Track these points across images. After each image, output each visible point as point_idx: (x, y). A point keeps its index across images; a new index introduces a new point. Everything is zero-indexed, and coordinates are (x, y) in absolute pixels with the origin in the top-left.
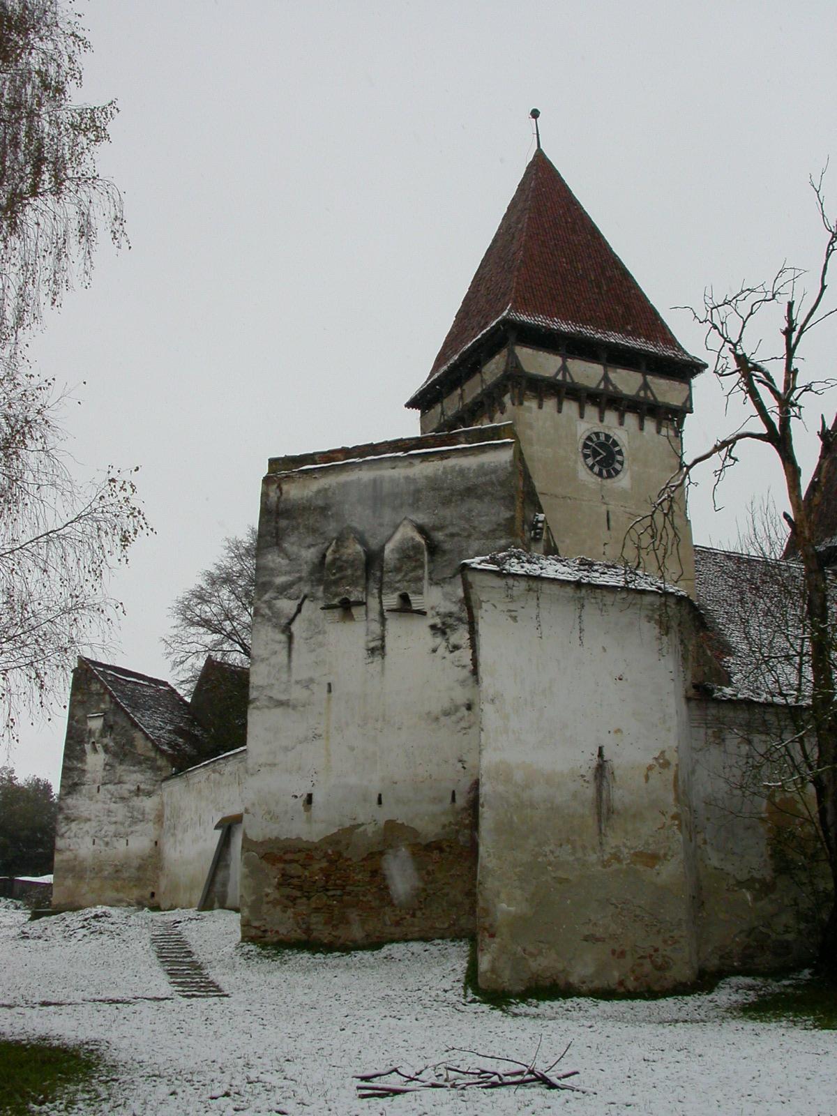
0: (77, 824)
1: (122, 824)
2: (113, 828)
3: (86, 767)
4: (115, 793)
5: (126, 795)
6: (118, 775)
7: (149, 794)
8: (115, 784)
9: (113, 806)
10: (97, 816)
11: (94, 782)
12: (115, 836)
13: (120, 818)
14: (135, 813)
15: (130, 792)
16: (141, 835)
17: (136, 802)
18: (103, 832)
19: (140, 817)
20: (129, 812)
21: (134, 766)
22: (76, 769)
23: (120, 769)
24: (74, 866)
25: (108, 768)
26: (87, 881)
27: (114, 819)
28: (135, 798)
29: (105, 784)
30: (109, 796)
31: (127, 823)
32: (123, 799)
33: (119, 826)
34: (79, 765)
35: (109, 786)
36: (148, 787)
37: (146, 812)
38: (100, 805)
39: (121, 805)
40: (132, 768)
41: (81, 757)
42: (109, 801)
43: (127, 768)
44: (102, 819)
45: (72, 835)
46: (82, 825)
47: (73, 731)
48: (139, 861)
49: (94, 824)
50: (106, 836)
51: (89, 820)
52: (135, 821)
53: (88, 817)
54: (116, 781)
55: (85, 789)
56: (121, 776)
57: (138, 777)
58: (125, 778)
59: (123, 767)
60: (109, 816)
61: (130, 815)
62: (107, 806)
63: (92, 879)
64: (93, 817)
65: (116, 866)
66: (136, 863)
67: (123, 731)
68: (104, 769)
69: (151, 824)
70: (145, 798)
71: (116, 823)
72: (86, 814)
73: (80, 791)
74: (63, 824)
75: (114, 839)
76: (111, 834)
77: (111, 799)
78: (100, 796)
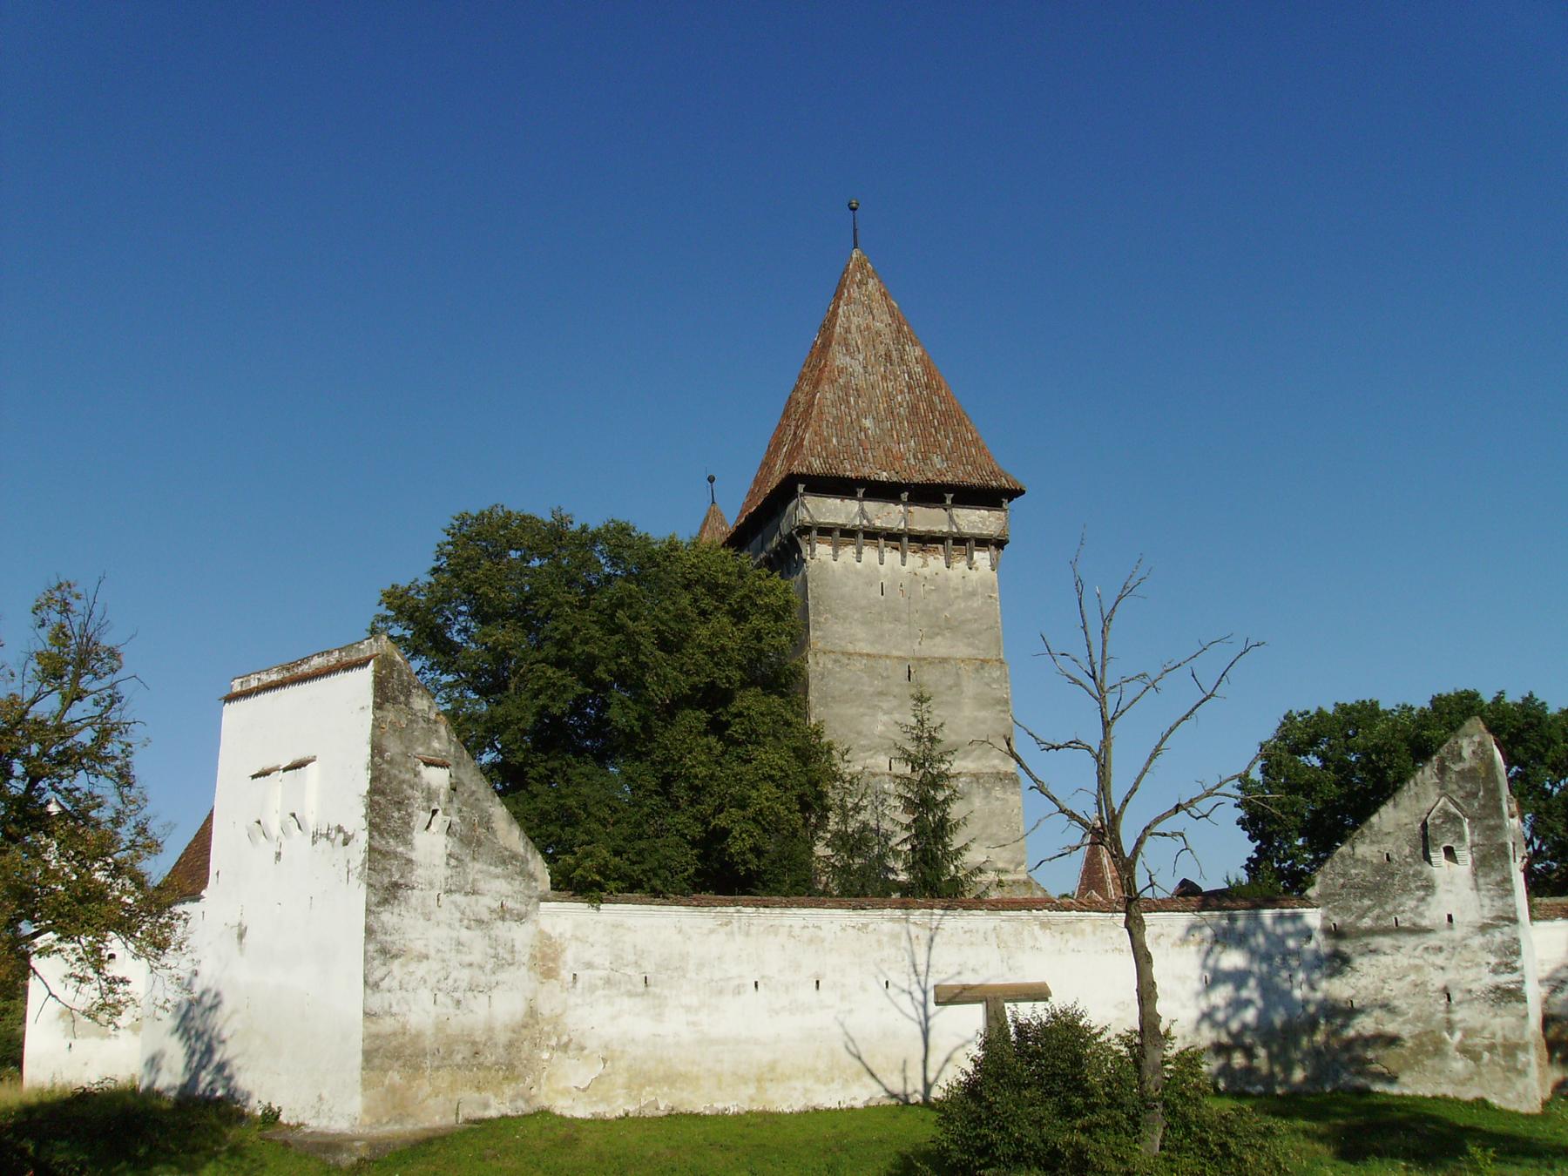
0: (402, 965)
1: (481, 968)
2: (465, 975)
3: (413, 855)
4: (467, 910)
5: (485, 916)
6: (470, 879)
7: (521, 918)
8: (467, 894)
9: (465, 934)
10: (439, 951)
11: (431, 885)
12: (471, 990)
13: (476, 957)
14: (501, 950)
15: (492, 911)
16: (511, 989)
17: (502, 929)
18: (450, 981)
19: (508, 957)
20: (491, 947)
21: (496, 867)
22: (396, 855)
23: (475, 868)
24: (402, 1045)
25: (453, 862)
26: (427, 1073)
27: (467, 959)
28: (499, 923)
29: (449, 891)
30: (458, 915)
31: (488, 967)
32: (480, 922)
33: (477, 972)
34: (400, 849)
35: (457, 897)
36: (518, 906)
37: (516, 948)
38: (443, 932)
39: (479, 933)
40: (492, 868)
41: (403, 833)
42: (457, 925)
43: (485, 867)
44: (447, 956)
45: (395, 984)
46: (413, 967)
47: (385, 779)
48: (510, 1035)
49: (434, 964)
50: (455, 990)
51: (427, 957)
52: (501, 964)
53: (424, 951)
54: (468, 888)
55: (415, 896)
56: (474, 880)
57: (502, 886)
58: (481, 885)
59: (478, 866)
60: (458, 951)
61: (492, 952)
62: (454, 934)
63: (438, 1068)
64: (432, 953)
65: (474, 1043)
66: (502, 1038)
67: (472, 800)
68: (448, 864)
69: (524, 970)
70: (514, 924)
71: (471, 965)
72: (419, 946)
73: (406, 900)
74: (376, 963)
75: (469, 994)
76: (464, 985)
77: (461, 921)
78: (442, 915)
